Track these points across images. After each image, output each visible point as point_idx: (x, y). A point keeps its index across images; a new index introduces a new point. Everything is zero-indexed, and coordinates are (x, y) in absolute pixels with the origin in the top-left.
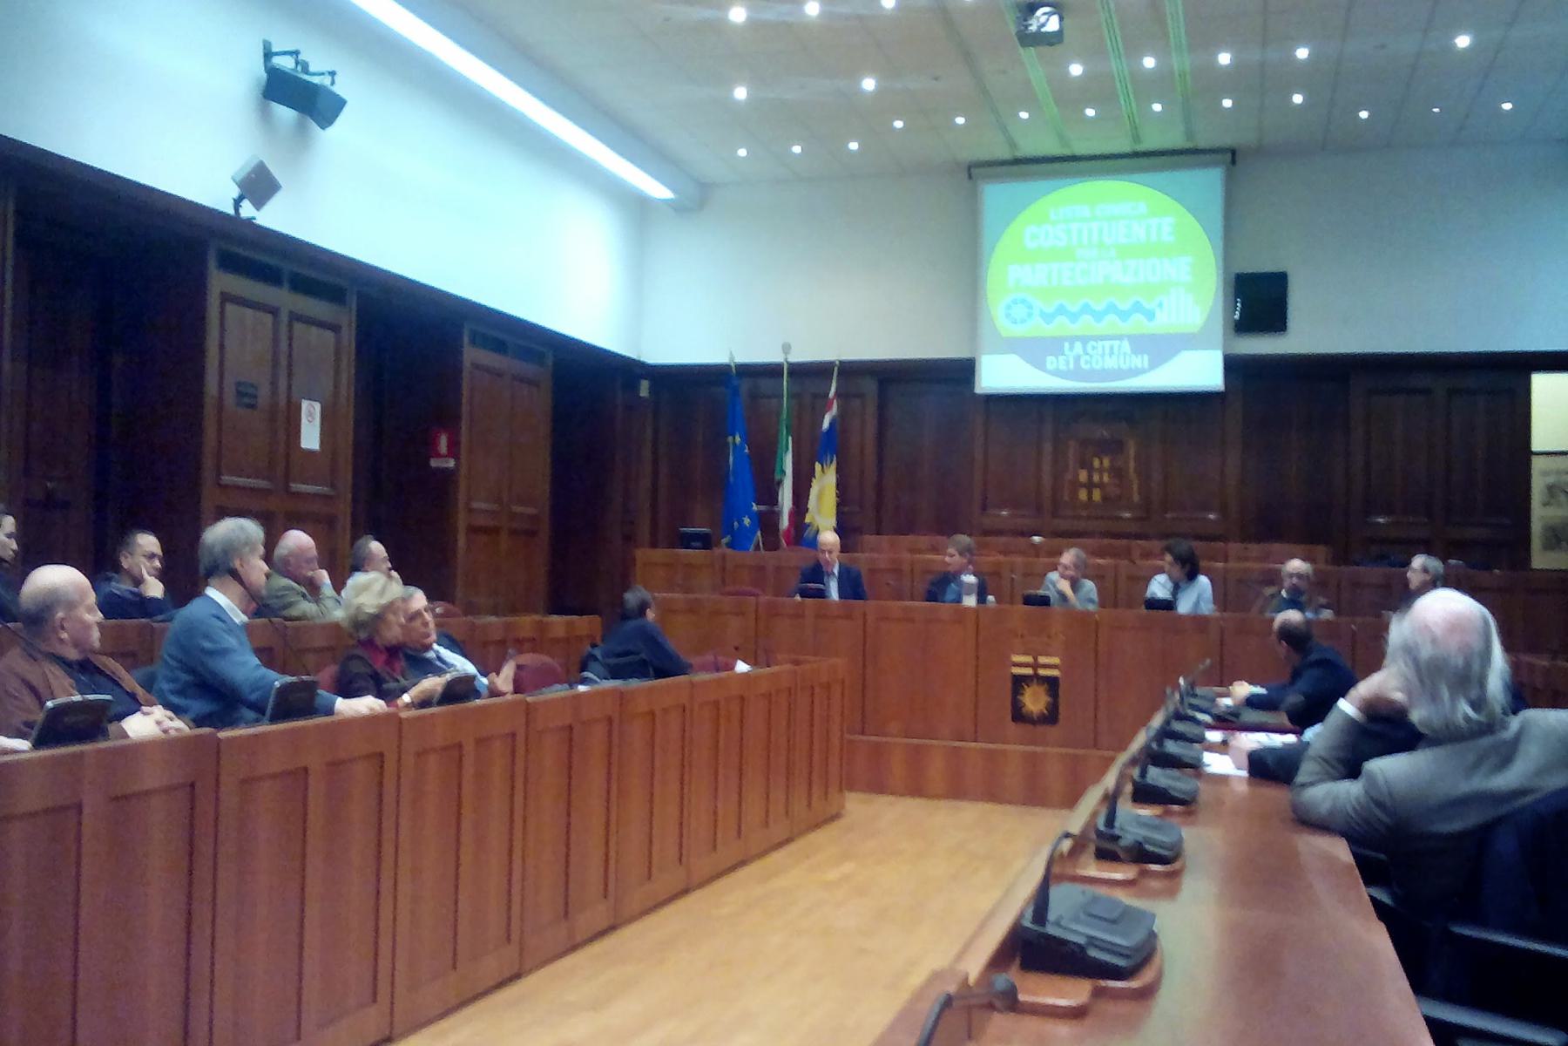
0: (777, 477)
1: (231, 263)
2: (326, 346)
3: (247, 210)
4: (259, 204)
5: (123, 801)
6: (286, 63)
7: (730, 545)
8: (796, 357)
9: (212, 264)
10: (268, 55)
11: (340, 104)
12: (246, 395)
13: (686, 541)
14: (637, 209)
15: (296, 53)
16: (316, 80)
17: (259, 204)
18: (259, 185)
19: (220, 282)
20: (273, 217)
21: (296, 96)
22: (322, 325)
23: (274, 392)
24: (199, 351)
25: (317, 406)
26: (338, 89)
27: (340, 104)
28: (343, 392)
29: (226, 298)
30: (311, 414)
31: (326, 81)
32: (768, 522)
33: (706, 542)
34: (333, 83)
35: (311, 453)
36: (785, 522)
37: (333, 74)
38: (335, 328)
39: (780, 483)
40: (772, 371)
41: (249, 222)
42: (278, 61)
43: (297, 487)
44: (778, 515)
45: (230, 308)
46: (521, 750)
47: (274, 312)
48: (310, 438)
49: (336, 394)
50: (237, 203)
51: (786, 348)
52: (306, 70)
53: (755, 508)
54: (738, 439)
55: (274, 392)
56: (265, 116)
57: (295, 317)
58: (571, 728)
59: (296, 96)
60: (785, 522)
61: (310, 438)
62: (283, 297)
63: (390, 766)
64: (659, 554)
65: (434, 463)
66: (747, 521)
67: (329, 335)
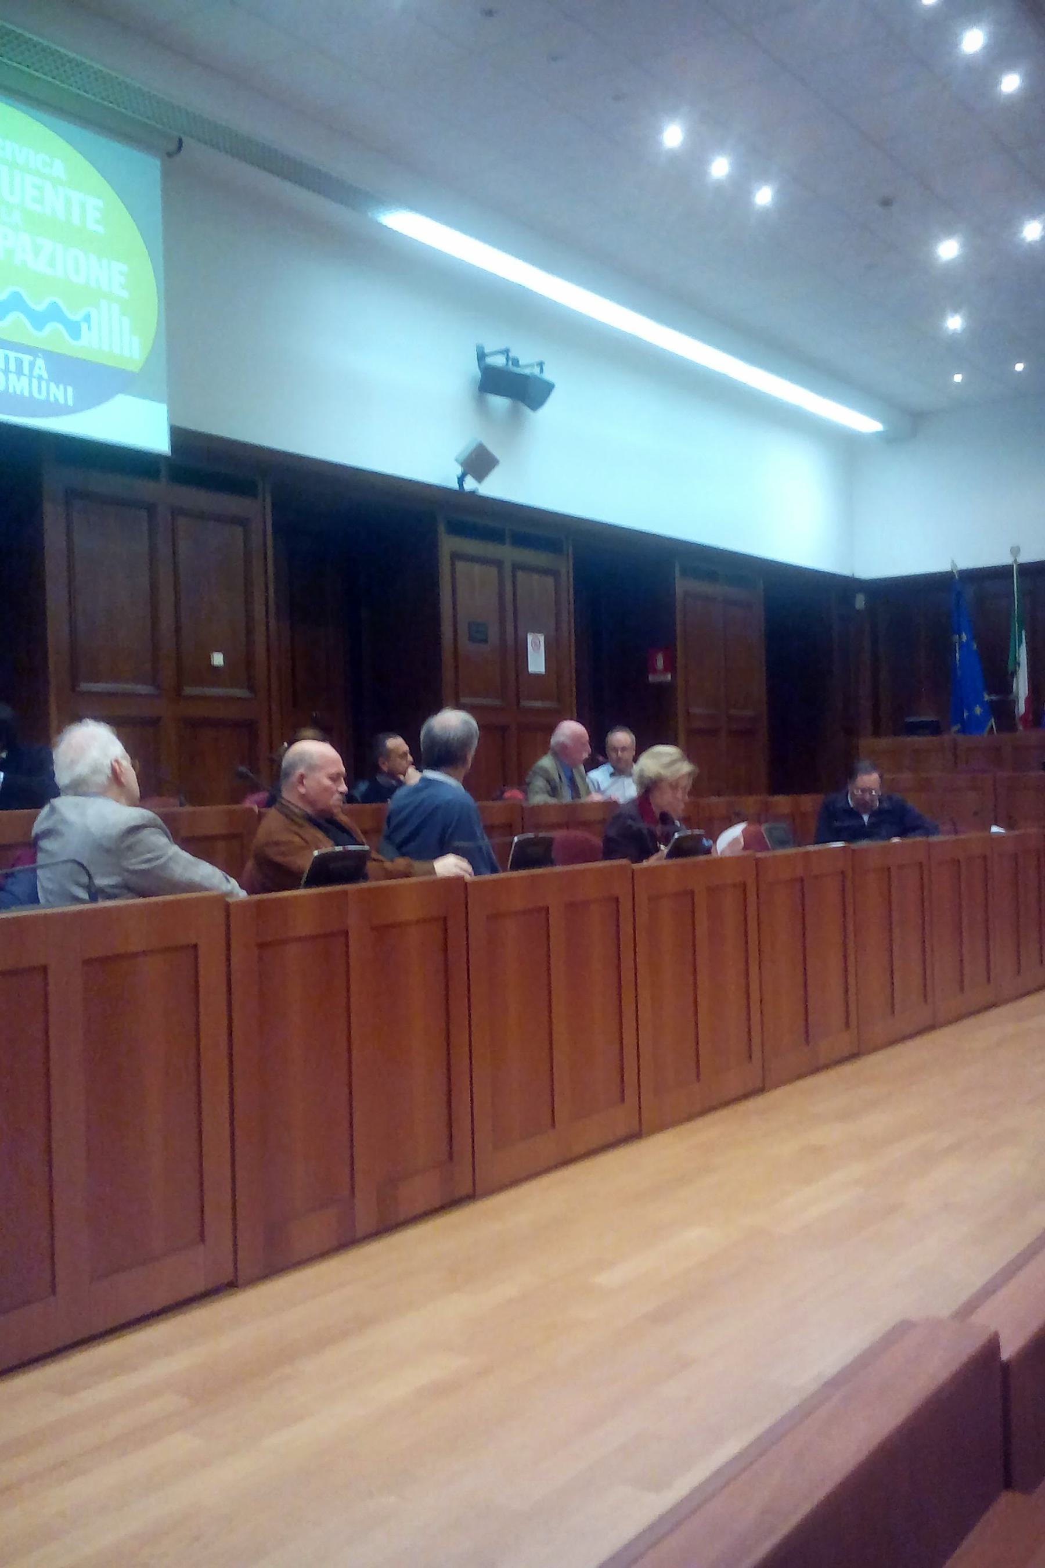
0: (1011, 668)
1: (459, 529)
2: (547, 588)
3: (470, 484)
4: (480, 477)
5: (384, 931)
6: (499, 361)
7: (963, 731)
8: (1025, 558)
9: (442, 528)
10: (481, 356)
11: (548, 388)
12: (477, 633)
13: (913, 729)
14: (846, 449)
15: (506, 352)
16: (527, 371)
17: (480, 477)
18: (479, 462)
19: (448, 544)
20: (493, 487)
21: (509, 388)
22: (545, 572)
23: (503, 632)
24: (435, 619)
25: (542, 638)
26: (548, 375)
27: (548, 388)
28: (565, 627)
29: (455, 556)
30: (536, 646)
31: (536, 371)
32: (1003, 711)
33: (935, 729)
34: (542, 370)
35: (537, 676)
36: (1021, 708)
37: (541, 365)
38: (554, 573)
39: (1014, 673)
40: (999, 574)
41: (473, 493)
42: (490, 361)
43: (526, 703)
44: (1014, 702)
45: (460, 565)
46: (752, 898)
47: (498, 564)
48: (537, 663)
49: (558, 628)
50: (461, 480)
51: (1015, 551)
52: (516, 362)
53: (987, 698)
54: (964, 638)
55: (503, 632)
56: (481, 404)
57: (516, 567)
58: (802, 880)
59: (509, 388)
60: (1021, 708)
61: (537, 663)
62: (508, 553)
63: (626, 906)
64: (884, 743)
65: (652, 678)
66: (978, 710)
67: (550, 581)
